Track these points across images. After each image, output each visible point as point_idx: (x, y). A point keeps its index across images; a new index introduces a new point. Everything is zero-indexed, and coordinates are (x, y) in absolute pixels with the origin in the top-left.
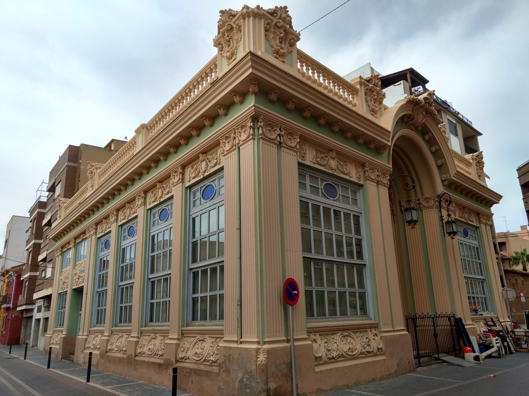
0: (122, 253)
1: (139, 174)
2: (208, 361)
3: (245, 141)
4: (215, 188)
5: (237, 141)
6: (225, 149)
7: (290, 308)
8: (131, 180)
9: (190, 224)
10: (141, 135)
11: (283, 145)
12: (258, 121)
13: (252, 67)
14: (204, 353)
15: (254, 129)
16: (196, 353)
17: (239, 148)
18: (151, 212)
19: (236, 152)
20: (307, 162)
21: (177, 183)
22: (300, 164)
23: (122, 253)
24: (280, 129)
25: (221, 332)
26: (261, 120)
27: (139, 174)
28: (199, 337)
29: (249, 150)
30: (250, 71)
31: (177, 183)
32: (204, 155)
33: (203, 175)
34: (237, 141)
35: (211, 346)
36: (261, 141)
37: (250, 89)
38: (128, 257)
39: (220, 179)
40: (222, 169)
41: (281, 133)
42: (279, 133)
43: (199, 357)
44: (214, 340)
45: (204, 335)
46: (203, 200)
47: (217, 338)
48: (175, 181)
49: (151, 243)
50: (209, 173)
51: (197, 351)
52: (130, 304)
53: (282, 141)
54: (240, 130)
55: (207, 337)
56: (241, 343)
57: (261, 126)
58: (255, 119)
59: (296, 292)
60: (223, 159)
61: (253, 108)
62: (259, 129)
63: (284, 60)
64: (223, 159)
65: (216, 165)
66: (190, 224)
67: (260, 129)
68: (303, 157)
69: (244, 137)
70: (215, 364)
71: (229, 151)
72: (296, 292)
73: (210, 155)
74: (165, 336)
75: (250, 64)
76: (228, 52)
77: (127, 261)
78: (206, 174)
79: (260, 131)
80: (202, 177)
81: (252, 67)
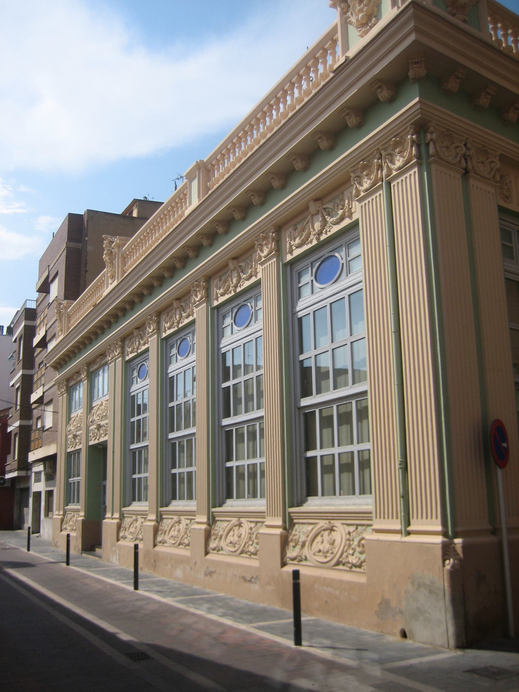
0: (167, 386)
1: (196, 249)
2: (344, 565)
3: (403, 170)
4: (342, 262)
5: (385, 172)
6: (361, 188)
7: (499, 472)
8: (183, 260)
9: (292, 331)
10: (196, 181)
11: (472, 174)
12: (426, 132)
13: (416, 29)
14: (335, 551)
15: (418, 146)
16: (320, 551)
17: (389, 184)
18: (218, 312)
19: (383, 193)
20: (513, 207)
21: (268, 258)
22: (501, 209)
23: (167, 386)
24: (465, 145)
25: (366, 515)
26: (431, 129)
27: (196, 249)
28: (323, 523)
29: (409, 188)
30: (412, 38)
31: (268, 258)
32: (318, 204)
33: (318, 239)
34: (385, 172)
35: (348, 540)
36: (433, 167)
37: (411, 74)
38: (181, 391)
39: (349, 246)
40: (355, 225)
41: (468, 153)
42: (463, 152)
43: (326, 557)
44: (352, 529)
45: (332, 521)
46: (316, 285)
47: (357, 525)
48: (262, 255)
49: (220, 368)
50: (329, 234)
51: (321, 547)
52: (189, 469)
53: (470, 167)
54: (389, 151)
55: (337, 523)
56: (409, 533)
57: (432, 140)
58: (421, 127)
59: (505, 445)
60: (356, 206)
61: (418, 106)
62: (428, 145)
63: (467, 19)
64: (356, 206)
65: (342, 219)
66: (292, 331)
67: (431, 145)
68: (507, 197)
69: (399, 162)
70: (358, 570)
71: (370, 192)
72: (505, 445)
73: (330, 201)
74: (257, 522)
75: (411, 25)
76: (361, 11)
77: (179, 398)
78: (323, 237)
79: (432, 150)
80: (315, 242)
81: (416, 29)
